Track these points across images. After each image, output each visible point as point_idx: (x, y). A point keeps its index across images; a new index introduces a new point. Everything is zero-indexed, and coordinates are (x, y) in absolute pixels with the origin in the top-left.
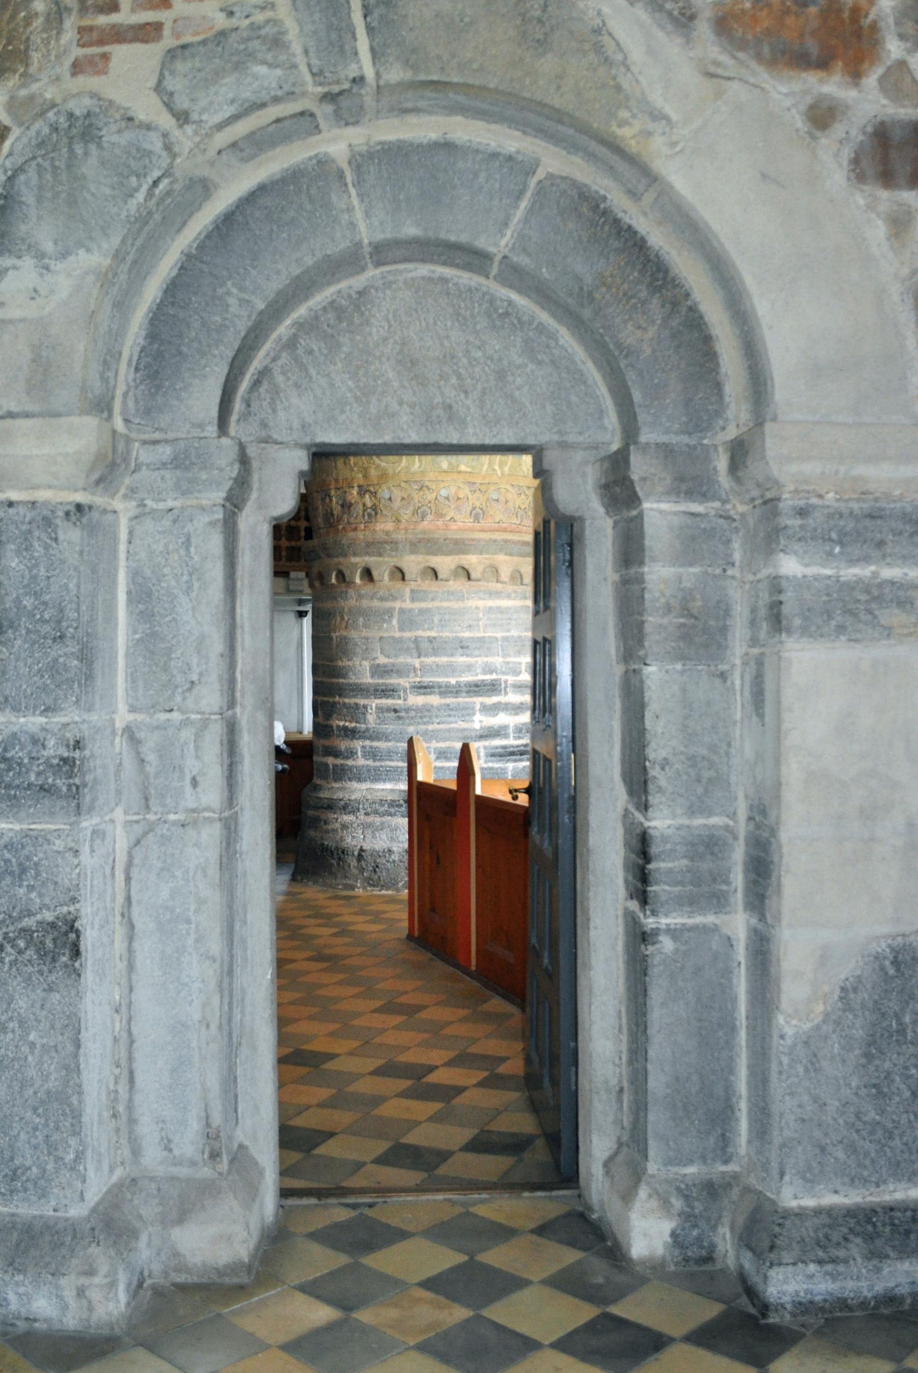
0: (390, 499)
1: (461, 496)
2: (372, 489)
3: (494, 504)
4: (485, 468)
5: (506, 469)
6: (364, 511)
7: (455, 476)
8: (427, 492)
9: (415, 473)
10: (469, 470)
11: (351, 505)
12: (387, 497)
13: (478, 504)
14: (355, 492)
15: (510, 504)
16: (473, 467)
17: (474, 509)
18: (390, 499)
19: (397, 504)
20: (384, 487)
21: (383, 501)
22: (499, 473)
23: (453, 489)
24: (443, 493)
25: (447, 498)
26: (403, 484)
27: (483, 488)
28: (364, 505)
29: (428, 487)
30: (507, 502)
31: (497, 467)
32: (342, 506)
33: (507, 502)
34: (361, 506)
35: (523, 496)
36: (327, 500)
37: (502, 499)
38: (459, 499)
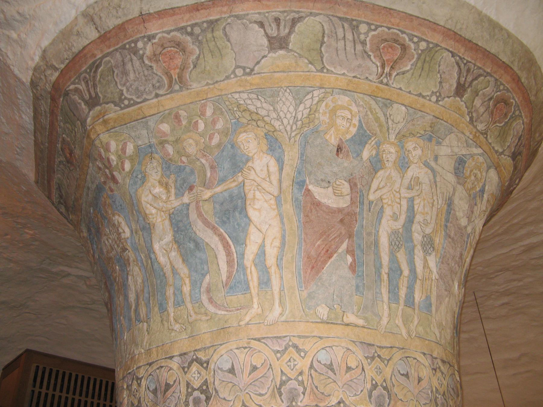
0: (232, 371)
1: (353, 365)
2: (202, 356)
3: (402, 380)
4: (385, 320)
5: (412, 327)
6: (189, 394)
7: (338, 331)
8: (295, 356)
9: (275, 323)
10: (361, 322)
11: (168, 386)
12: (228, 366)
13: (379, 379)
14: (175, 364)
15: (424, 383)
16: (366, 319)
17: (375, 386)
18: (232, 371)
19: (244, 379)
20: (222, 350)
21: (220, 375)
22: (404, 332)
23: (339, 353)
24: (323, 357)
25: (330, 367)
26: (254, 344)
27: (385, 354)
28: (188, 385)
29: (296, 347)
30: (420, 380)
31: (399, 322)
32: (155, 392)
33: (420, 380)
34: (183, 389)
35: (439, 374)
36: (135, 386)
37: (413, 374)
38: (349, 369)
